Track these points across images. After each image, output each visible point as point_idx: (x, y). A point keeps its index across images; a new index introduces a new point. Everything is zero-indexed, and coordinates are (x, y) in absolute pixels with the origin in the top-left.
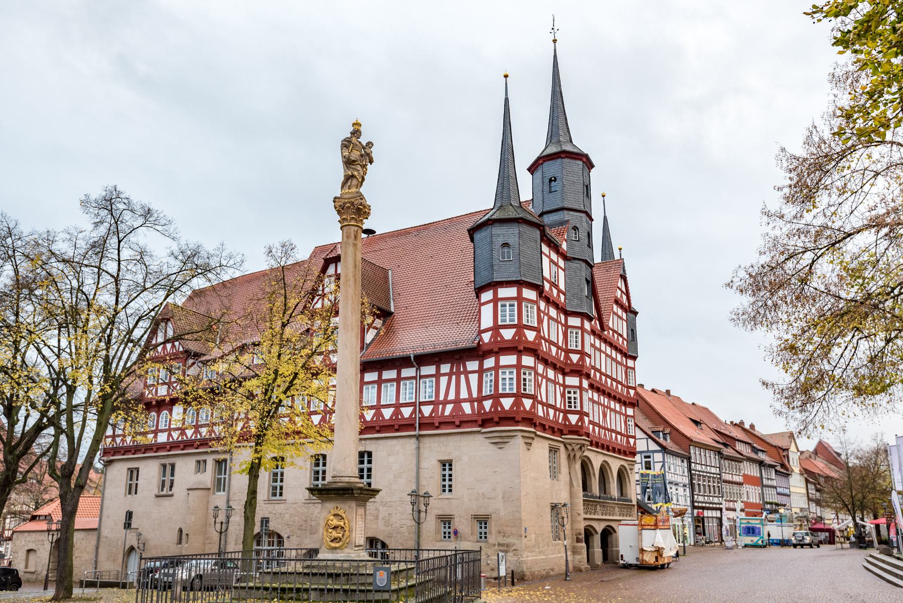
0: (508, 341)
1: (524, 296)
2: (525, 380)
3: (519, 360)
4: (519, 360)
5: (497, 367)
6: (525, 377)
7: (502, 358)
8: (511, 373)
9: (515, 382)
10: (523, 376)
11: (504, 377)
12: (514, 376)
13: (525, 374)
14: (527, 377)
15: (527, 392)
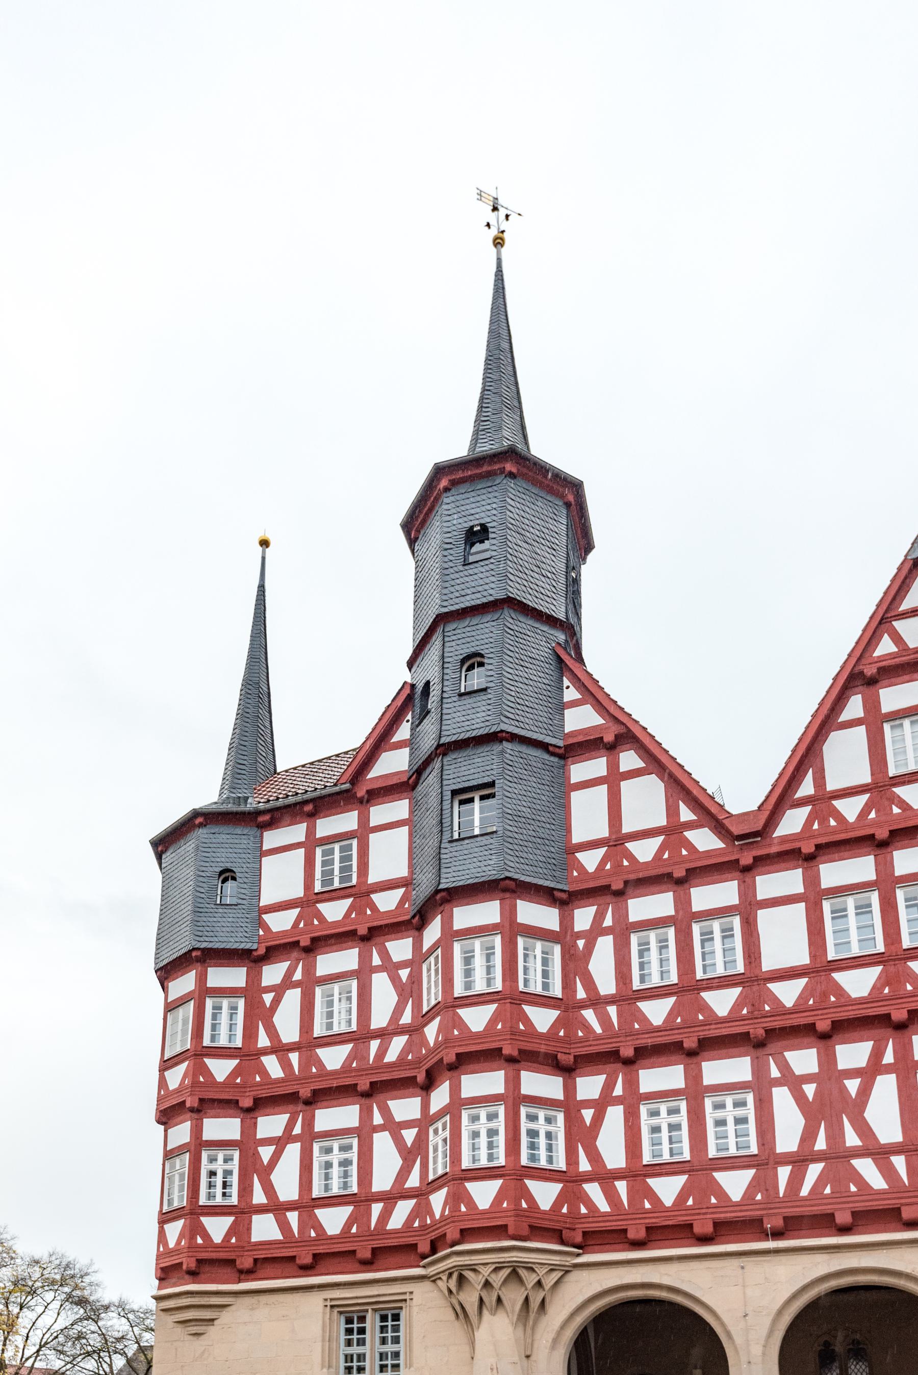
0: (478, 1035)
1: (521, 919)
2: (533, 1134)
3: (513, 1083)
4: (513, 1083)
5: (457, 1105)
6: (532, 1126)
7: (465, 1079)
8: (491, 1117)
9: (501, 1140)
10: (525, 1125)
11: (475, 1127)
12: (500, 1124)
13: (532, 1118)
14: (541, 1126)
15: (543, 1163)
